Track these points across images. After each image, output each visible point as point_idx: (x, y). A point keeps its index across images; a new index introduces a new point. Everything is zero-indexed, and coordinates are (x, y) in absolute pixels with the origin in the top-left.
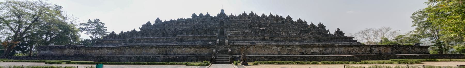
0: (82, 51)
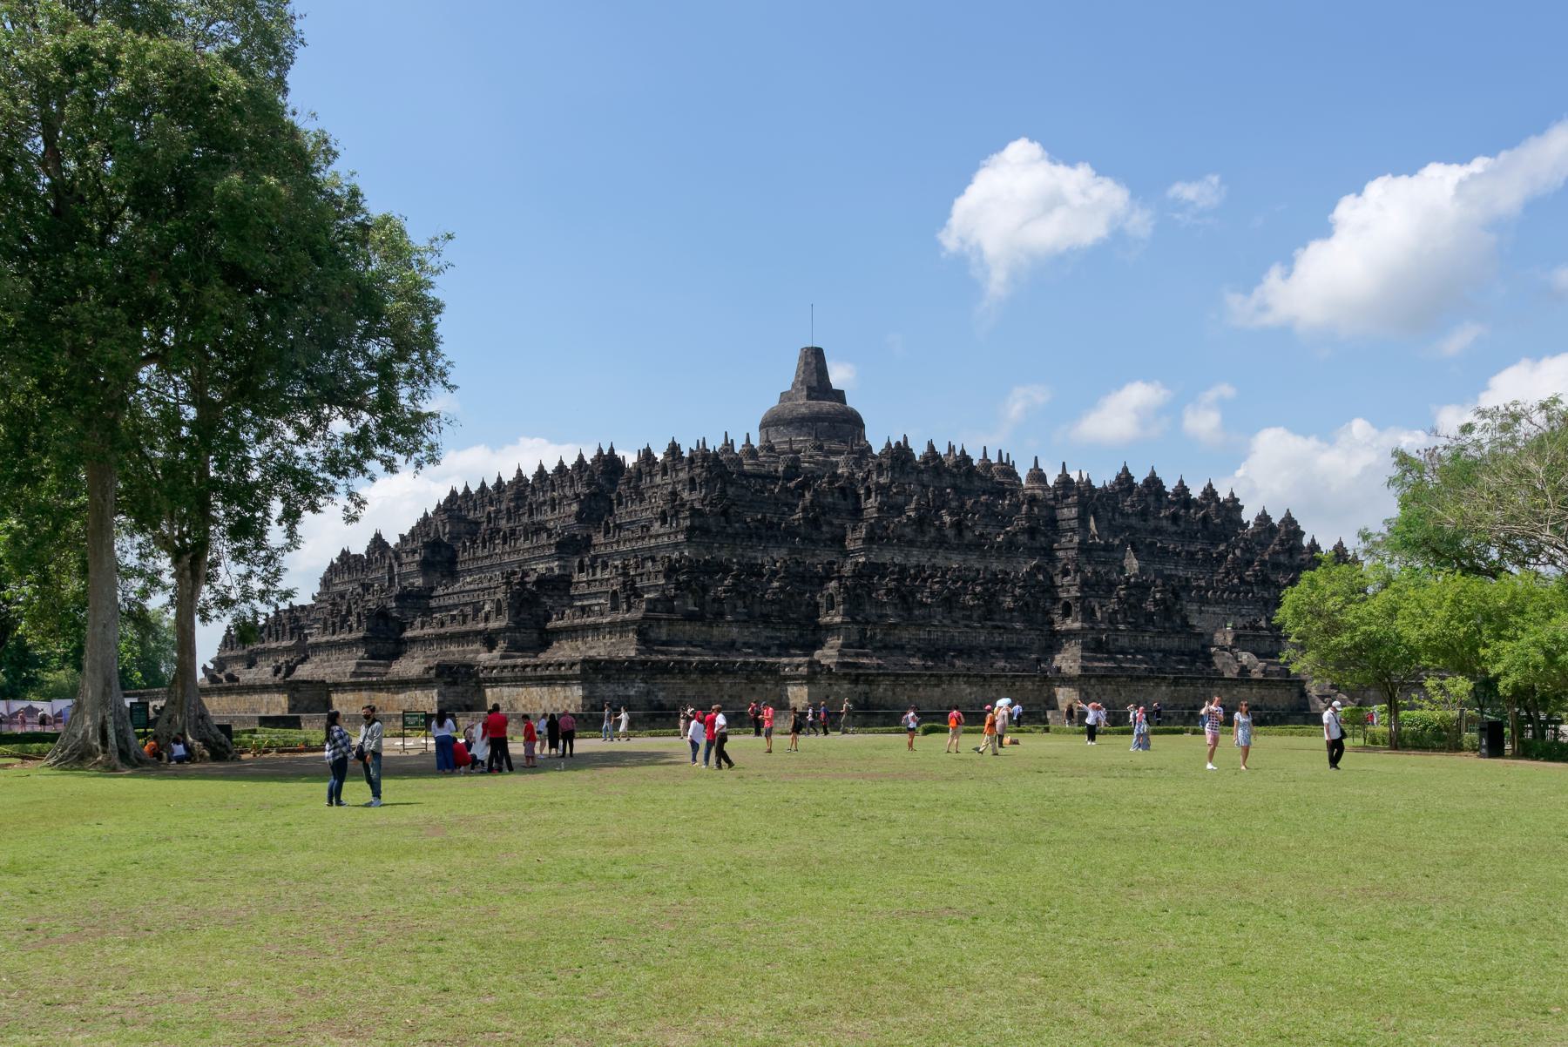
0: (881, 690)
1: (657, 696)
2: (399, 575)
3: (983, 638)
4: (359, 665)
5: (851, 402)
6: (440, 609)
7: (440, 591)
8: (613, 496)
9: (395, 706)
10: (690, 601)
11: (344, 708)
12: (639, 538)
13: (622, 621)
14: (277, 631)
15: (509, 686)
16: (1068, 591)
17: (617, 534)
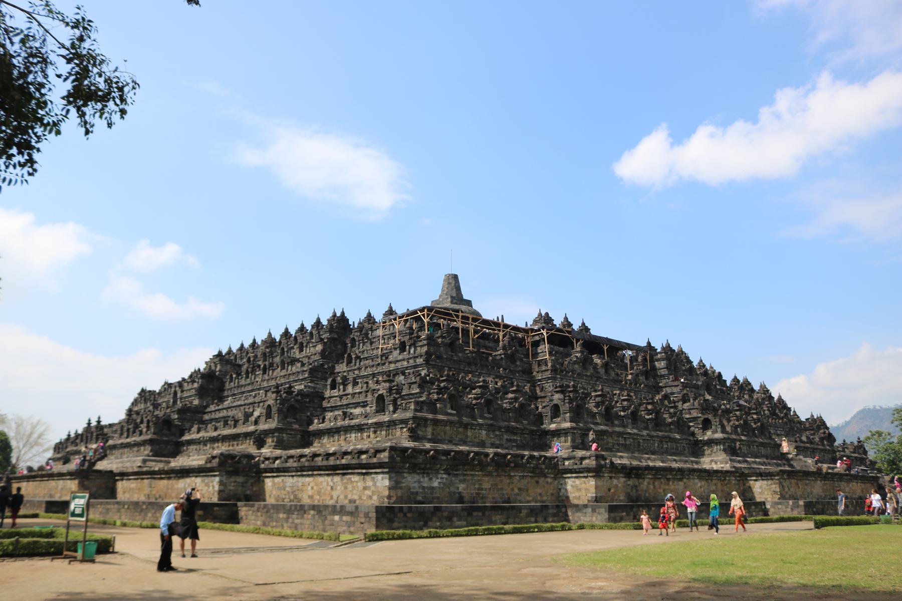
0: (645, 483)
1: (458, 488)
2: (181, 399)
3: (656, 445)
4: (144, 461)
5: (476, 306)
6: (211, 420)
7: (212, 408)
8: (348, 341)
9: (173, 495)
10: (449, 406)
11: (127, 495)
12: (378, 364)
13: (389, 421)
14: (87, 437)
15: (293, 476)
16: (690, 413)
17: (358, 364)
